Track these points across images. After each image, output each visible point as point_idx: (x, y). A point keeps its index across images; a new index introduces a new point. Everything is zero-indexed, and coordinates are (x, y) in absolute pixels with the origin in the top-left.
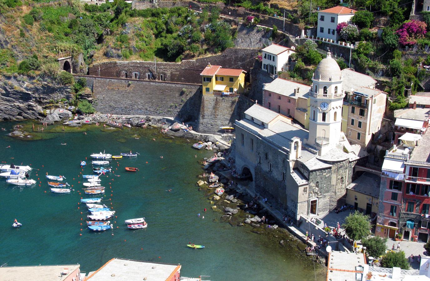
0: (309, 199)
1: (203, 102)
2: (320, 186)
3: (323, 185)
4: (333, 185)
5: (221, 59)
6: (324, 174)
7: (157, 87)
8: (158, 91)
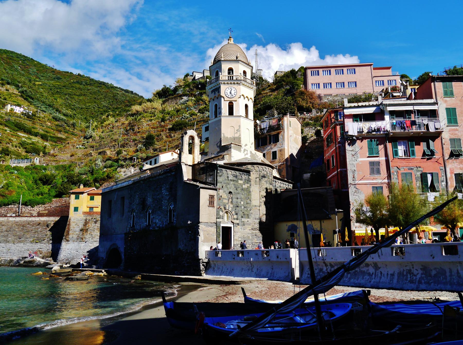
0: (218, 220)
1: (69, 225)
2: (235, 200)
3: (239, 200)
4: (256, 206)
6: (240, 182)
7: (16, 222)
8: (17, 227)
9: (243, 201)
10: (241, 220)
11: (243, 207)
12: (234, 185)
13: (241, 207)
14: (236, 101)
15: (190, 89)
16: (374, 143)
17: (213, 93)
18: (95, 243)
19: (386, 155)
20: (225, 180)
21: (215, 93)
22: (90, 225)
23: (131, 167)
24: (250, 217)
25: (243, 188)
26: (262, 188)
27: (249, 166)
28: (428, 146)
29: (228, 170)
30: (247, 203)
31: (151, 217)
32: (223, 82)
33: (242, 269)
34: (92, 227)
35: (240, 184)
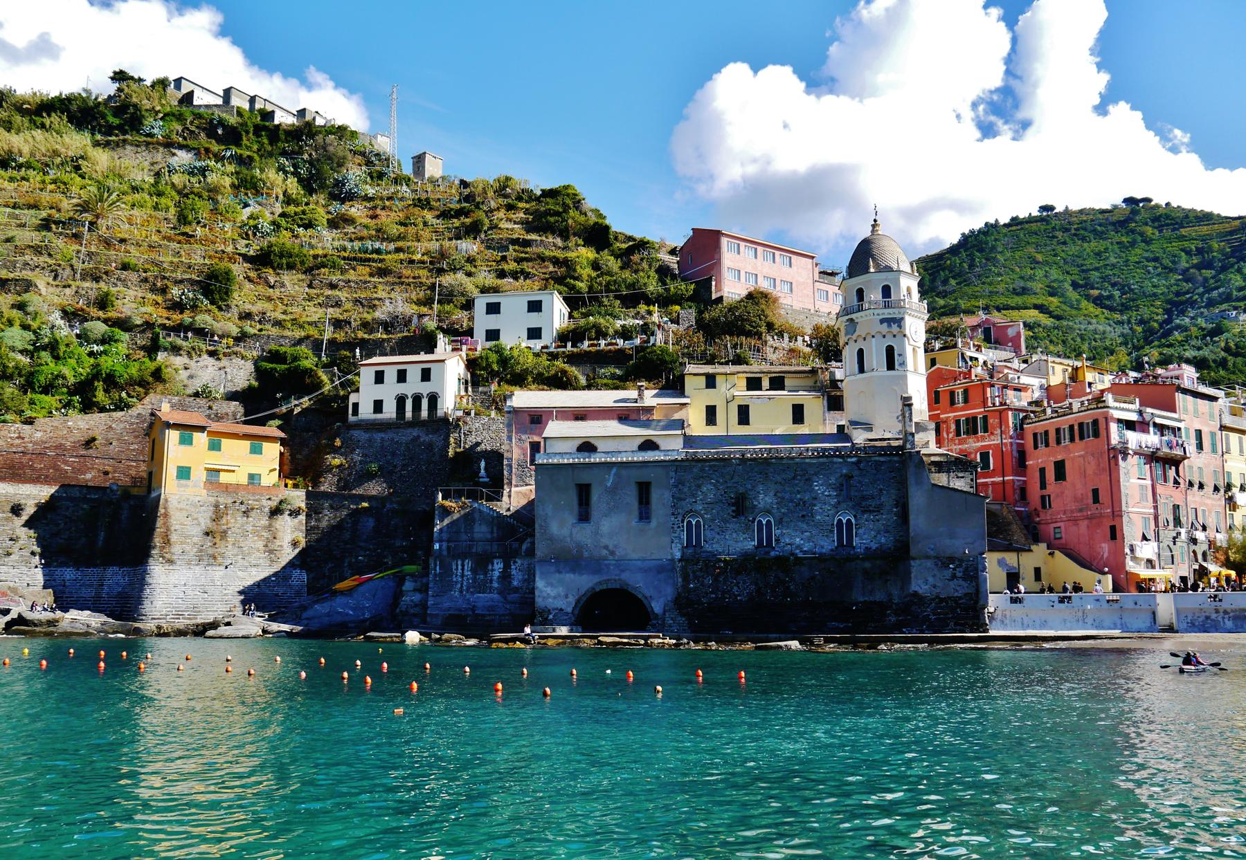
1: (166, 515)
5: (132, 424)
15: (188, 129)
16: (1142, 461)
17: (885, 324)
18: (254, 569)
19: (1152, 480)
21: (889, 326)
22: (233, 521)
23: (205, 356)
28: (1177, 472)
31: (776, 532)
33: (1065, 621)
34: (238, 525)
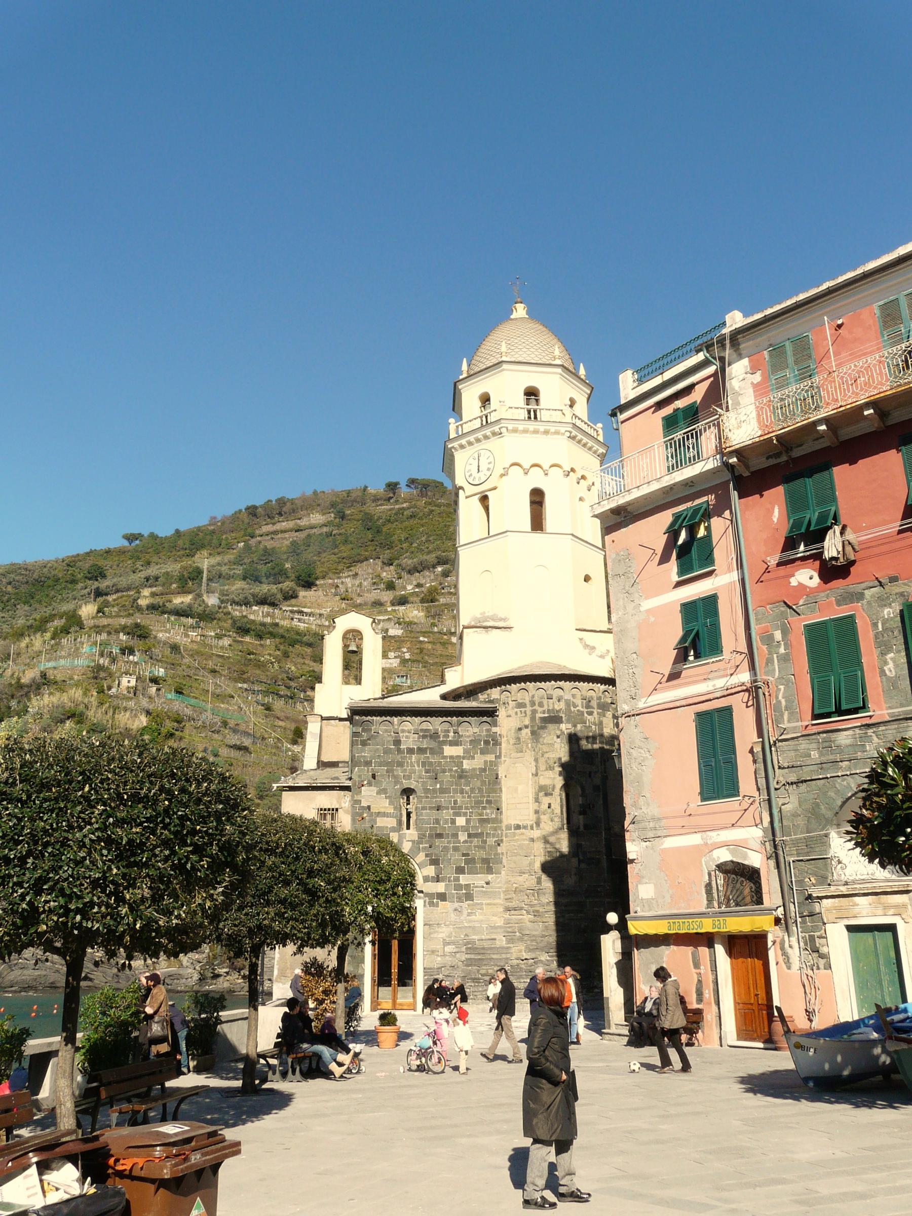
3: (446, 814)
4: (518, 827)
6: (449, 751)
9: (465, 814)
10: (457, 879)
11: (463, 837)
12: (424, 764)
13: (455, 835)
14: (495, 488)
20: (387, 751)
24: (495, 867)
25: (463, 771)
26: (542, 761)
27: (495, 693)
29: (396, 720)
30: (483, 821)
32: (456, 444)
35: (451, 757)
